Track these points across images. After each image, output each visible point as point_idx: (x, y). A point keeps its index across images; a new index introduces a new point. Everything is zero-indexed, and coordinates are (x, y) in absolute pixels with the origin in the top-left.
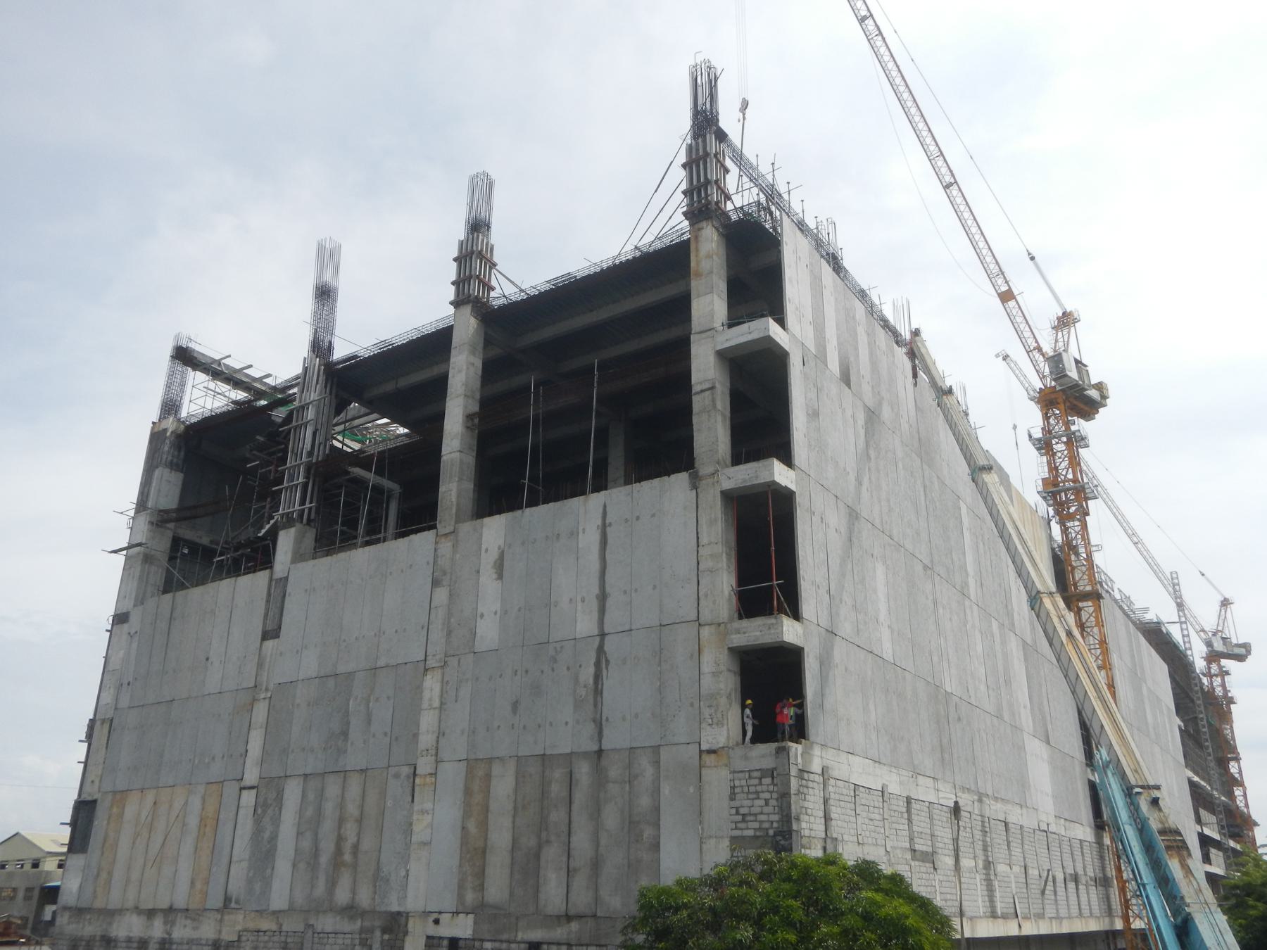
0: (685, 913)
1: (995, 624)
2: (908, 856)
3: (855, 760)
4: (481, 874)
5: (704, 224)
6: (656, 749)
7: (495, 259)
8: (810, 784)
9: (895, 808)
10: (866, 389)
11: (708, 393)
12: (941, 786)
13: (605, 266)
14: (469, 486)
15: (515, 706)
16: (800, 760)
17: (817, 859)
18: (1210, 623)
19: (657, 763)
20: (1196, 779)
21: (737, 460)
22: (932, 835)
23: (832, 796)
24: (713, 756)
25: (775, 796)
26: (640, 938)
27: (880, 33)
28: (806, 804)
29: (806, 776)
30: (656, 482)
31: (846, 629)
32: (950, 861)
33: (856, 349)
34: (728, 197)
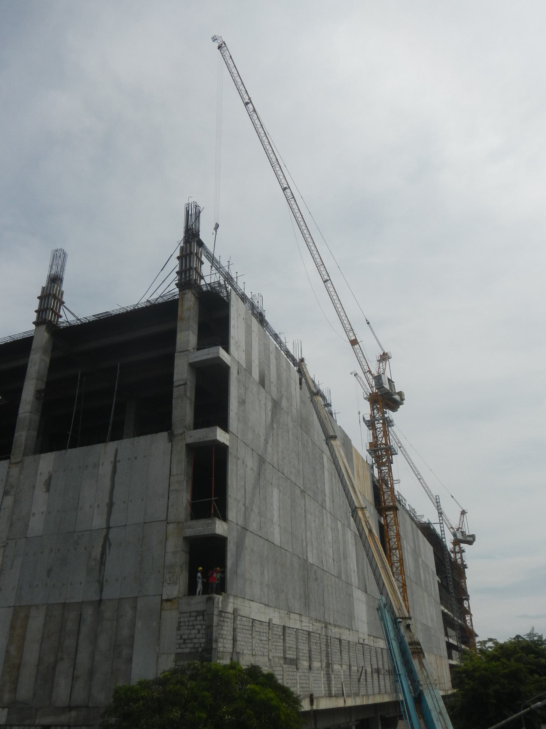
0: (141, 702)
1: (339, 524)
2: (282, 662)
3: (254, 605)
4: (15, 682)
5: (187, 291)
6: (135, 599)
7: (64, 299)
8: (226, 620)
9: (276, 633)
10: (274, 390)
11: (182, 387)
12: (304, 620)
13: (129, 309)
14: (35, 433)
15: (49, 571)
16: (220, 605)
17: (225, 666)
18: (455, 524)
19: (135, 608)
20: (446, 611)
21: (197, 425)
22: (297, 648)
23: (239, 626)
24: (169, 603)
25: (204, 627)
26: (113, 720)
27: (294, 197)
28: (222, 632)
29: (223, 614)
30: (149, 437)
31: (253, 526)
32: (306, 664)
33: (269, 367)
34: (202, 278)
